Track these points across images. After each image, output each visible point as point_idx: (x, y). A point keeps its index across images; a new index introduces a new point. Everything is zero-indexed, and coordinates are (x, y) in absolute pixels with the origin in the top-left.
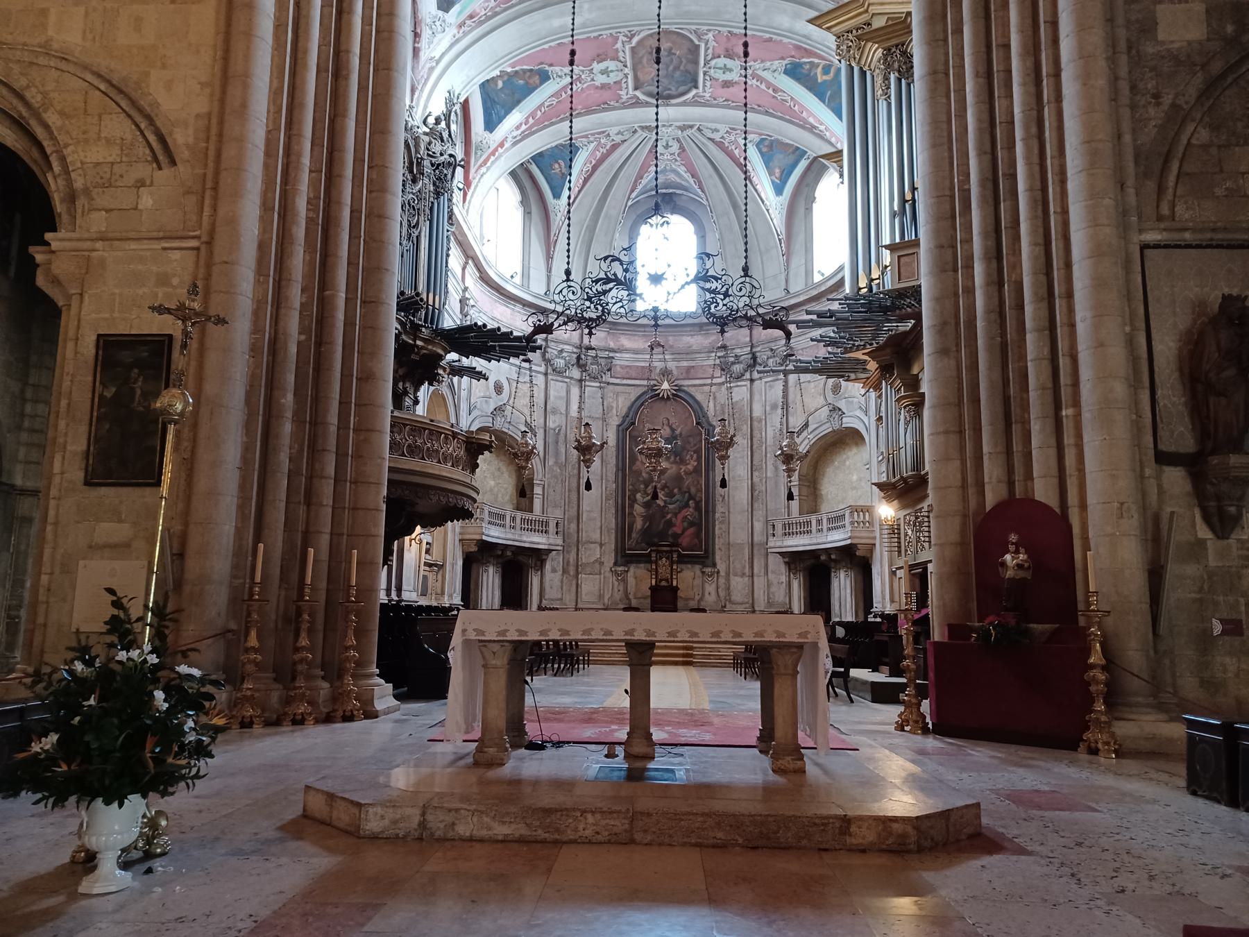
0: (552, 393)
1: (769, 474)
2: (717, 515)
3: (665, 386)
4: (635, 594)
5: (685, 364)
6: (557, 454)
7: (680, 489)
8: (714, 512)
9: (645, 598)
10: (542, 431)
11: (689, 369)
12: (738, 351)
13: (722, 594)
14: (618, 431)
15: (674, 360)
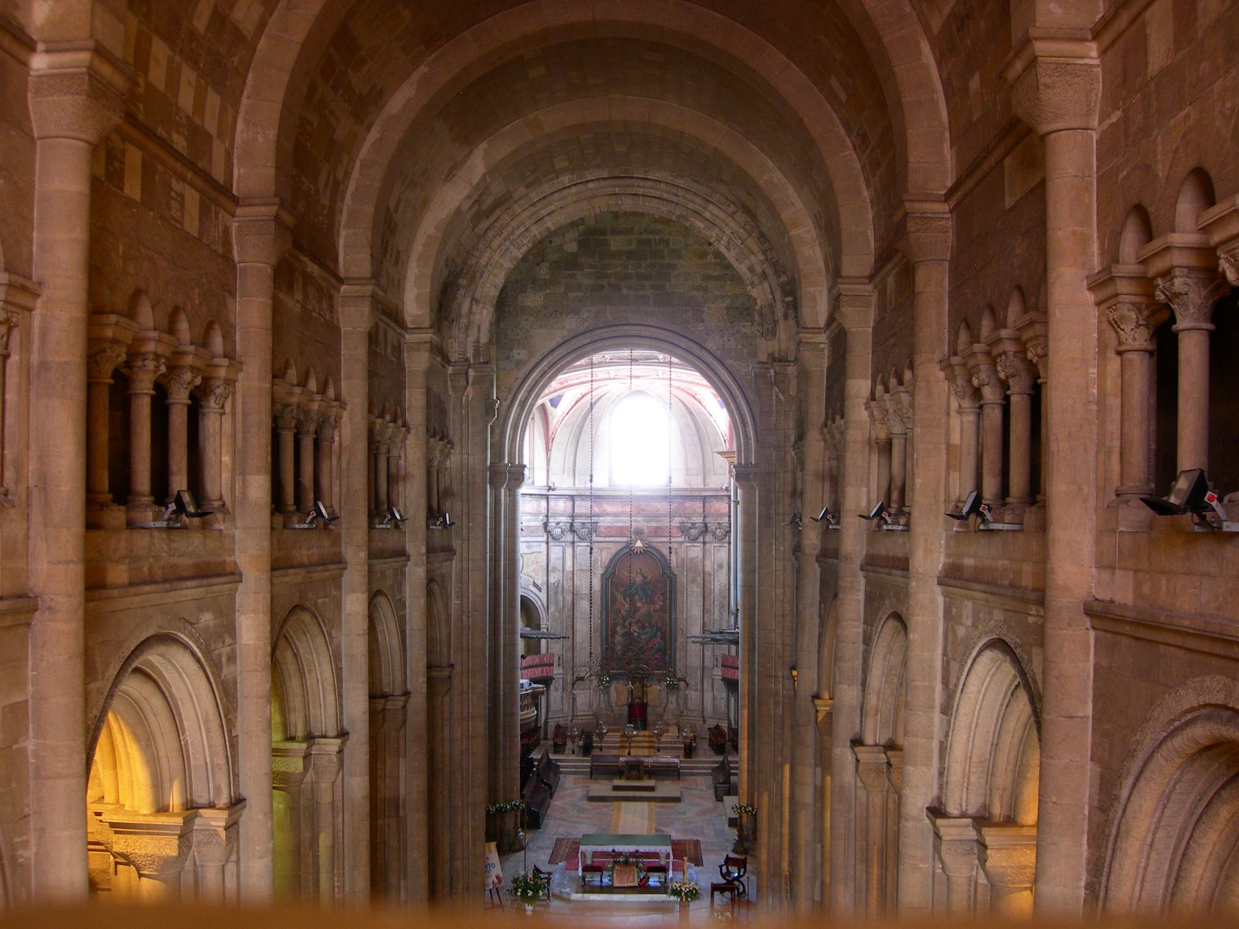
0: (552, 556)
1: (716, 617)
2: (678, 644)
3: (639, 544)
4: (616, 703)
5: (654, 524)
6: (557, 603)
7: (650, 624)
8: (676, 641)
9: (623, 706)
10: (545, 586)
11: (657, 528)
12: (694, 519)
13: (681, 702)
14: (602, 579)
15: (645, 521)
